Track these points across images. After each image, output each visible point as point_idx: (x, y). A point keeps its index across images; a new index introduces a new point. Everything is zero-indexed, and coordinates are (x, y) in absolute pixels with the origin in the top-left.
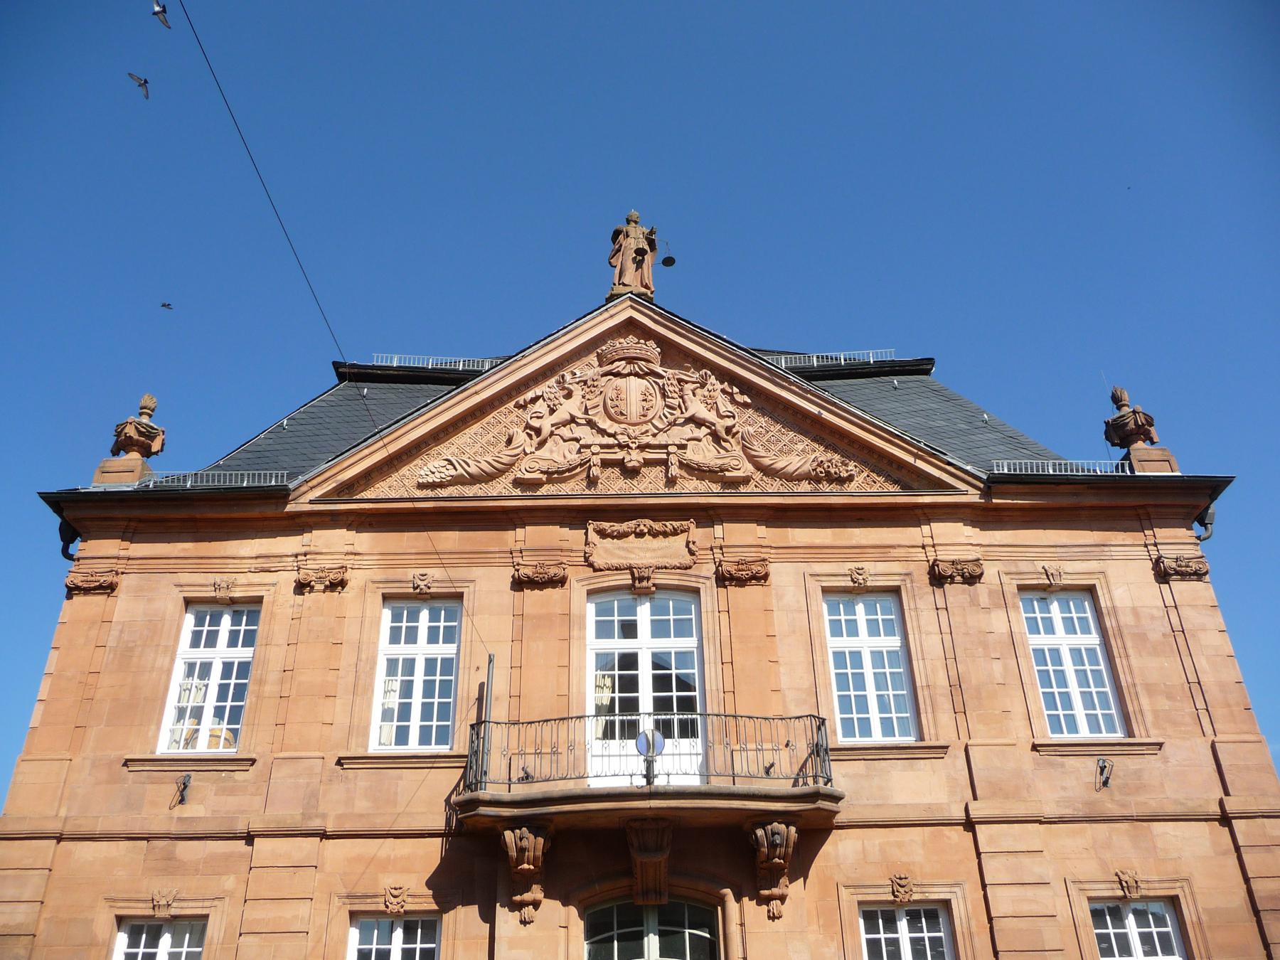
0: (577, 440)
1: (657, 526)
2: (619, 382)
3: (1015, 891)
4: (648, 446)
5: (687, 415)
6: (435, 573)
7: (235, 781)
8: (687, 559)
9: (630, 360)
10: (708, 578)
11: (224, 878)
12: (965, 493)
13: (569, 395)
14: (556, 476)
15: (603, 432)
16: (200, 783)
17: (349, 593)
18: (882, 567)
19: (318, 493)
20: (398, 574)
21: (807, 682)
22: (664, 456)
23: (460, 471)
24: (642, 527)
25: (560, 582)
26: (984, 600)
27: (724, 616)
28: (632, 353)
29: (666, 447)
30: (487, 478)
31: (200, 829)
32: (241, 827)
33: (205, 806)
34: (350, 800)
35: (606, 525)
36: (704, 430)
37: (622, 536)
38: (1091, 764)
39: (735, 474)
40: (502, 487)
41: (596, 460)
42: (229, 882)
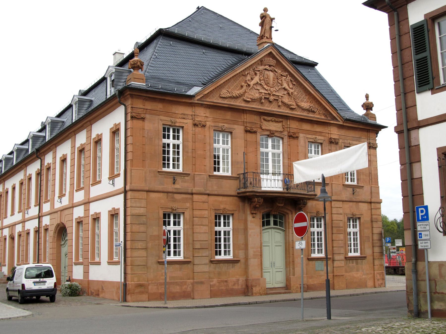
0: (259, 90)
1: (277, 120)
2: (267, 72)
5: (283, 87)
6: (226, 125)
8: (282, 130)
12: (340, 122)
13: (256, 74)
14: (253, 100)
16: (179, 179)
17: (206, 129)
20: (217, 124)
25: (255, 132)
27: (289, 146)
29: (279, 96)
30: (236, 98)
31: (180, 191)
32: (190, 191)
33: (180, 185)
34: (213, 187)
37: (269, 121)
39: (292, 107)
42: (188, 205)
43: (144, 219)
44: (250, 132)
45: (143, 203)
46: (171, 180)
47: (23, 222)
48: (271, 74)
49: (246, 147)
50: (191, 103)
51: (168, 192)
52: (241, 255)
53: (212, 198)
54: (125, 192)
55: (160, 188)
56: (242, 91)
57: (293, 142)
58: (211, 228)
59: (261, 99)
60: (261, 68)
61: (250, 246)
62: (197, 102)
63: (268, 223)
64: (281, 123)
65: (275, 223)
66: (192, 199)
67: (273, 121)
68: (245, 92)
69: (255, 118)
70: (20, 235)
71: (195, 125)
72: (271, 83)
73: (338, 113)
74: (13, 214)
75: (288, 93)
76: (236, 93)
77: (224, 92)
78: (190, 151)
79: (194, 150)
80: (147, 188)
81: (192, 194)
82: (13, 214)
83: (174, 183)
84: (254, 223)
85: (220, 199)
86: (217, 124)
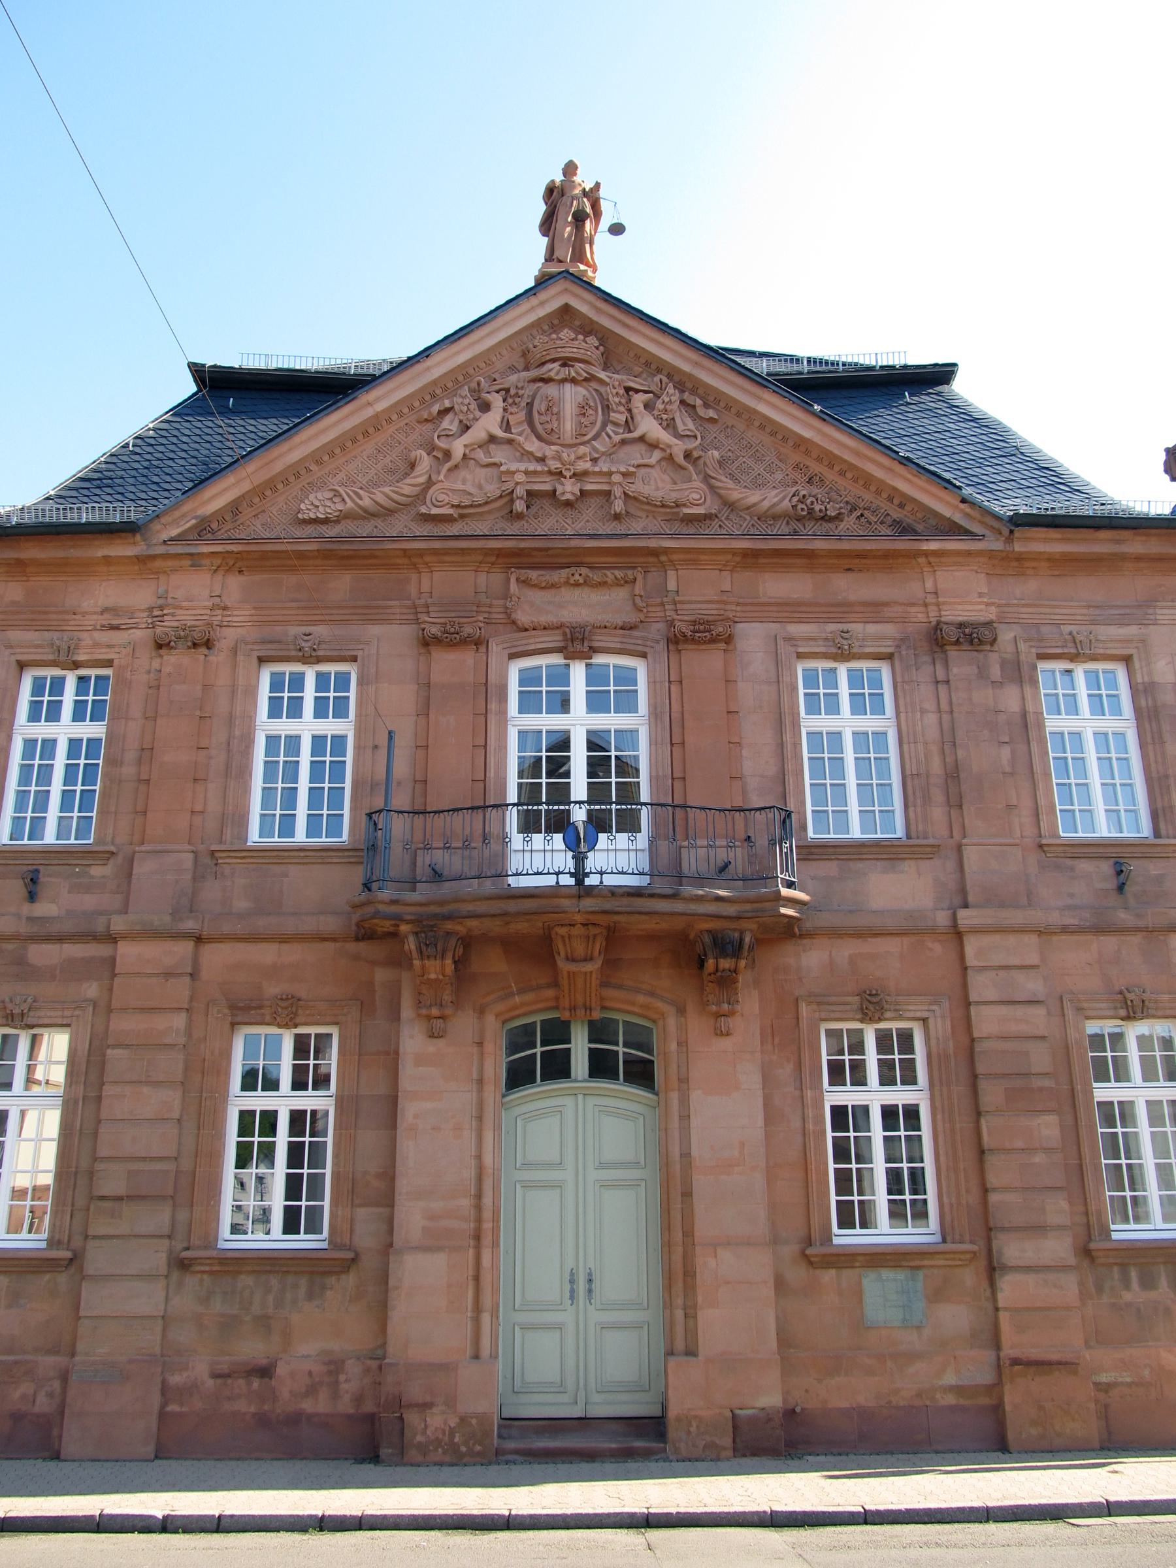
0: (497, 465)
1: (596, 576)
2: (551, 390)
3: (1003, 1010)
4: (585, 473)
5: (636, 434)
6: (320, 631)
7: (92, 877)
8: (632, 617)
9: (566, 362)
10: (658, 642)
11: (85, 985)
13: (485, 407)
15: (528, 455)
17: (219, 657)
18: (872, 629)
19: (174, 532)
21: (772, 770)
22: (606, 487)
23: (350, 504)
24: (577, 577)
26: (996, 672)
27: (675, 688)
28: (567, 353)
29: (610, 474)
31: (54, 929)
35: (534, 575)
36: (657, 455)
38: (1106, 867)
40: (400, 525)
41: (520, 491)
50: (141, 560)
52: (366, 1238)
57: (704, 663)
62: (161, 550)
64: (627, 588)
67: (577, 585)
68: (430, 483)
73: (964, 501)
75: (670, 458)
78: (130, 756)
79: (147, 752)
83: (32, 897)
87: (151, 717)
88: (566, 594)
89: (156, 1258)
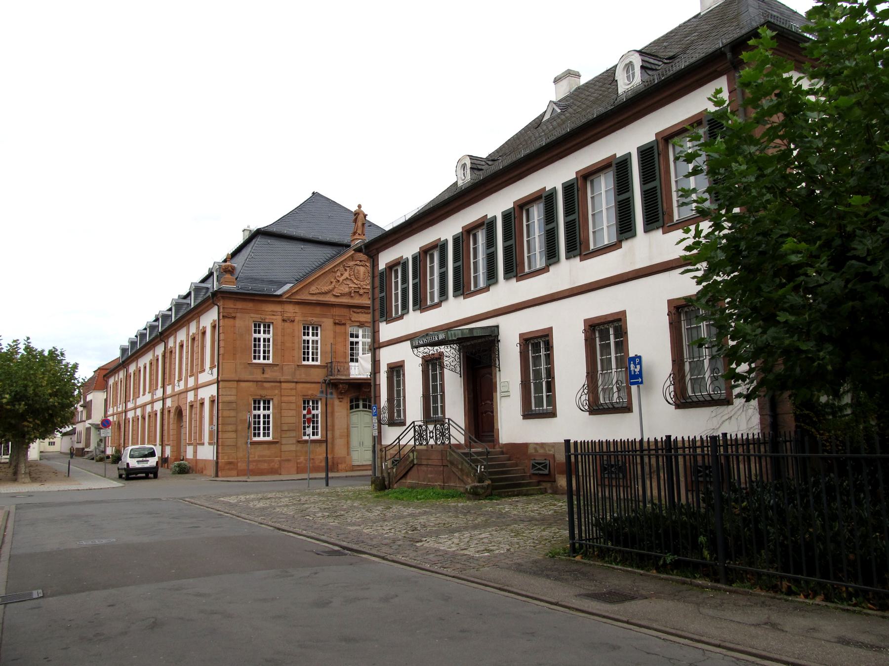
2: (358, 267)
14: (343, 295)
20: (305, 319)
25: (344, 324)
30: (326, 293)
33: (269, 375)
34: (301, 375)
42: (277, 392)
43: (234, 405)
44: (338, 324)
45: (234, 392)
46: (259, 371)
47: (152, 402)
48: (362, 269)
49: (335, 338)
51: (257, 382)
53: (300, 386)
54: (218, 382)
55: (250, 377)
56: (331, 287)
58: (299, 412)
59: (350, 293)
60: (351, 263)
61: (336, 427)
63: (357, 406)
65: (365, 406)
66: (280, 386)
69: (345, 311)
70: (149, 416)
71: (284, 320)
72: (362, 276)
74: (144, 394)
76: (325, 289)
77: (313, 289)
78: (279, 344)
80: (237, 379)
81: (280, 382)
82: (144, 394)
84: (340, 408)
85: (308, 385)
86: (305, 319)
87: (283, 336)
88: (360, 315)
89: (294, 442)
